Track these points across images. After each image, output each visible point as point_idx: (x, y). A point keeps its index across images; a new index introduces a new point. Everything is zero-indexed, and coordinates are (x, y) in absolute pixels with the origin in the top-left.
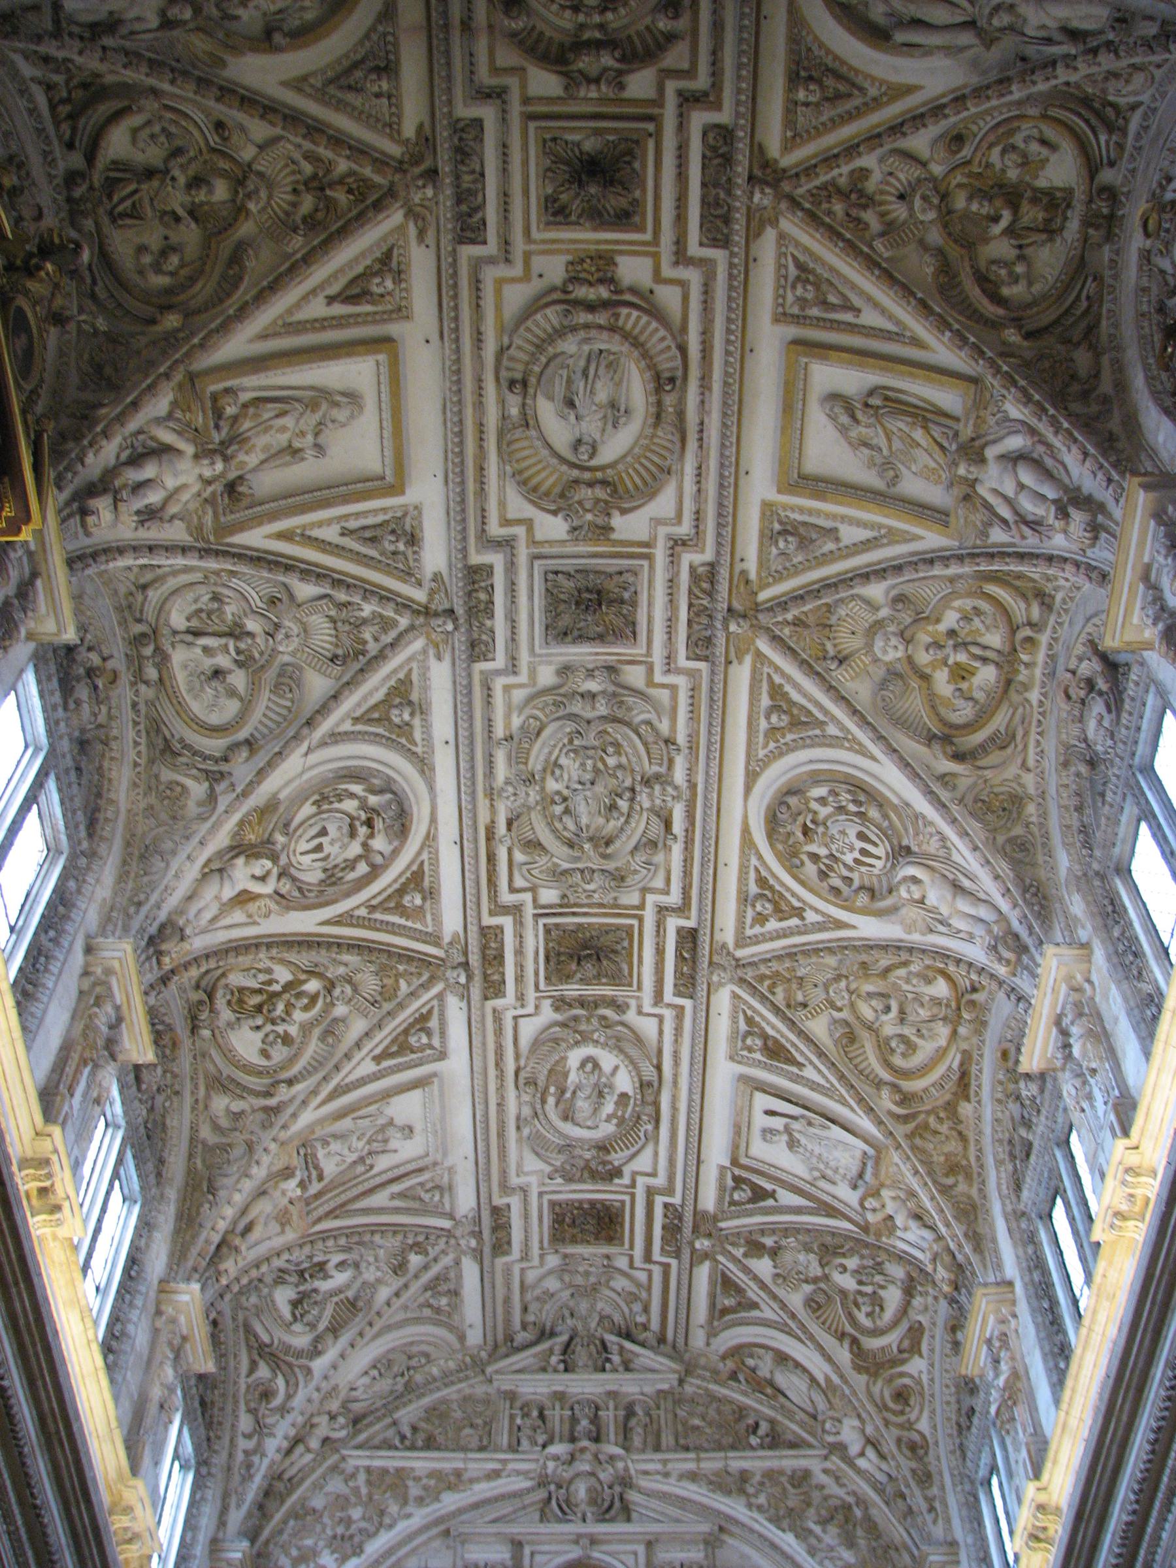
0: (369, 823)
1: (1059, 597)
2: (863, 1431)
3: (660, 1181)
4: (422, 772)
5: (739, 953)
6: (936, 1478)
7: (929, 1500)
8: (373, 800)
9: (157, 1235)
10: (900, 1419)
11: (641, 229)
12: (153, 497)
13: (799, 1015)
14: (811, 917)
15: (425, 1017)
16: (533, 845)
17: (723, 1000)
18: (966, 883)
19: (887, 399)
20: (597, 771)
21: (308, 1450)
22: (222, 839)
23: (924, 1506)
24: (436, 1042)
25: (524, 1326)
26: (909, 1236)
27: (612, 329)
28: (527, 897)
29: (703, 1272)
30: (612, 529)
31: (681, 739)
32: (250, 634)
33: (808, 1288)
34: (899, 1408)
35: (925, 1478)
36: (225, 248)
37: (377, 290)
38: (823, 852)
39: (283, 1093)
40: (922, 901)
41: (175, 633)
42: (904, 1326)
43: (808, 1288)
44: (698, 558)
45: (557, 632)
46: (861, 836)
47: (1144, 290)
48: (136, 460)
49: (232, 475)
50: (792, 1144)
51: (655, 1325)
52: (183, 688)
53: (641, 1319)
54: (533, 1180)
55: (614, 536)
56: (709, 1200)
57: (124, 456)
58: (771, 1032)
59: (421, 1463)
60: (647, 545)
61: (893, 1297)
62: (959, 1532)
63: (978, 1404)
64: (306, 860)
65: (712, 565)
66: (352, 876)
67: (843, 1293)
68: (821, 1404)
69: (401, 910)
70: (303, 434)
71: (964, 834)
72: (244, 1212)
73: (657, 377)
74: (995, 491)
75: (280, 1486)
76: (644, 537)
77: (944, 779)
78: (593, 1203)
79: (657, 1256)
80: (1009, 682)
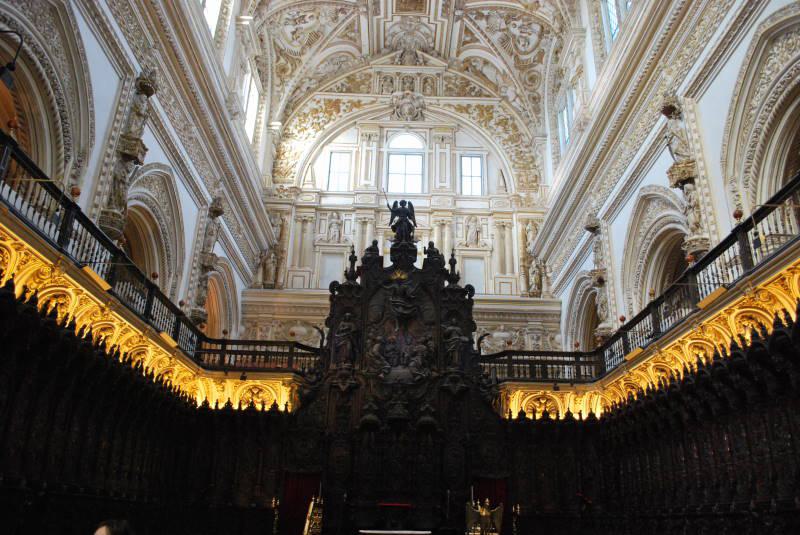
2: (516, 93)
7: (538, 119)
21: (301, 92)
25: (385, 47)
26: (544, 10)
33: (500, 34)
35: (537, 110)
42: (536, 51)
51: (437, 48)
53: (432, 45)
59: (345, 98)
61: (534, 39)
63: (563, 81)
67: (514, 36)
79: (439, 18)
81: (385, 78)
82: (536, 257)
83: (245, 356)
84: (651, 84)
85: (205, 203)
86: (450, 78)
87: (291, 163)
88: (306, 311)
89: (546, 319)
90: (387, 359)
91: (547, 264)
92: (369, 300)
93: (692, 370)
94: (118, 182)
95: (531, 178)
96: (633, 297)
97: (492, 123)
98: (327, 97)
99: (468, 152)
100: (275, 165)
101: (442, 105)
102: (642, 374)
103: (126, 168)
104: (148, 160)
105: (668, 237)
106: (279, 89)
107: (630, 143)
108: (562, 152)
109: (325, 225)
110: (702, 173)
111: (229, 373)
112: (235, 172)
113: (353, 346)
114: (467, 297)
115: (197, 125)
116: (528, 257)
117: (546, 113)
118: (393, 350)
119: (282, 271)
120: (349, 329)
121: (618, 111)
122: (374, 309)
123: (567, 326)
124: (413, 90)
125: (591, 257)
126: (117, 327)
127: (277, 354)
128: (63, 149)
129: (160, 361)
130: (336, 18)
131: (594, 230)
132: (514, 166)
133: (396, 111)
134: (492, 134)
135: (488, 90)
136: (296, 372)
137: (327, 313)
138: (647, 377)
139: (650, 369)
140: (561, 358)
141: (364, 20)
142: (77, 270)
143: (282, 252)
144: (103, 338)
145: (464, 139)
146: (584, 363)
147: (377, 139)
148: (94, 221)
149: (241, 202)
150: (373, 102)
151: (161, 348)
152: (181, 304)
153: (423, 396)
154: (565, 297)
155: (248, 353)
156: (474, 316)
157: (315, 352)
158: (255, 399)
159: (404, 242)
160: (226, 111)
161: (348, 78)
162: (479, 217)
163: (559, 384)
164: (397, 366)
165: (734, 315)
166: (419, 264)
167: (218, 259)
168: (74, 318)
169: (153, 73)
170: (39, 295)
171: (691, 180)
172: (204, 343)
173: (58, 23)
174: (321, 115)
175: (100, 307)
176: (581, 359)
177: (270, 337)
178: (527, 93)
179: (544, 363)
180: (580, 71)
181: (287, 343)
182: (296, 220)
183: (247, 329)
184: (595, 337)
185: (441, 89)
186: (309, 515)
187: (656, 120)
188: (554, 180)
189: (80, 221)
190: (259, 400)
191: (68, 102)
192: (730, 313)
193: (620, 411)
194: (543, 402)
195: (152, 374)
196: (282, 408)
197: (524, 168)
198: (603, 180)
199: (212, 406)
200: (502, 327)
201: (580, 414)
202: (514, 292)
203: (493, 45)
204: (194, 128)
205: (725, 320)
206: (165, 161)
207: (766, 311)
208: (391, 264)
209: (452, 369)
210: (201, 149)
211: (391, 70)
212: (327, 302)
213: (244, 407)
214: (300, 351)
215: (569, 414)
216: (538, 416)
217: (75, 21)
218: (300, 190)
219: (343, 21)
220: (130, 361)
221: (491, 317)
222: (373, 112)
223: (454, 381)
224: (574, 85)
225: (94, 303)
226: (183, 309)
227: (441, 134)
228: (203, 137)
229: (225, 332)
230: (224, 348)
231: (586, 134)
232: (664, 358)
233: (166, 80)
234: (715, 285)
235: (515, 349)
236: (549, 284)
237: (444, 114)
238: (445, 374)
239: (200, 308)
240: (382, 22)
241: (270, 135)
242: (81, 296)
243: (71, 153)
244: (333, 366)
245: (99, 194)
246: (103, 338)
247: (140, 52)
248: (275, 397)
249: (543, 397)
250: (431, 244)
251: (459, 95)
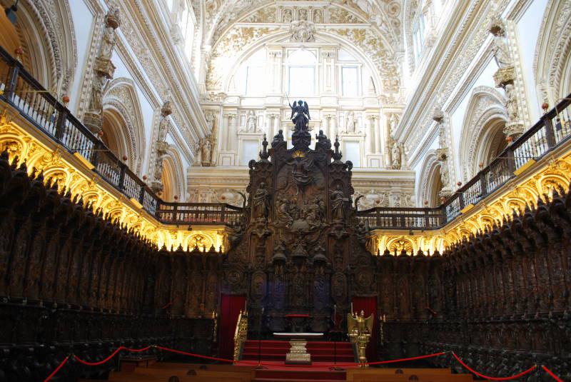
6: (401, 32)
21: (225, 23)
34: (392, 12)
35: (398, 32)
62: (406, 47)
75: (218, 33)
82: (397, 140)
83: (190, 214)
84: (483, 11)
85: (159, 106)
86: (333, 9)
88: (232, 182)
89: (403, 184)
90: (291, 215)
91: (405, 145)
92: (278, 173)
93: (509, 220)
94: (96, 92)
95: (394, 83)
96: (467, 167)
97: (365, 42)
98: (244, 26)
99: (347, 65)
100: (207, 77)
101: (328, 30)
102: (473, 223)
103: (101, 82)
104: (116, 75)
105: (496, 122)
106: (209, 21)
107: (466, 55)
108: (416, 63)
109: (244, 120)
110: (520, 76)
111: (180, 226)
112: (179, 83)
113: (266, 205)
114: (347, 170)
115: (150, 49)
116: (391, 141)
117: (405, 34)
118: (294, 208)
119: (215, 154)
120: (263, 194)
121: (458, 31)
122: (281, 180)
123: (419, 191)
124: (306, 20)
125: (437, 140)
126: (100, 195)
127: (213, 212)
128: (55, 69)
129: (131, 219)
131: (439, 119)
132: (380, 74)
133: (294, 35)
134: (365, 51)
135: (362, 18)
136: (227, 225)
137: (247, 183)
138: (477, 225)
139: (479, 220)
140: (415, 213)
142: (70, 155)
143: (214, 140)
144: (90, 203)
145: (346, 55)
146: (432, 216)
148: (80, 120)
149: (184, 105)
150: (277, 29)
151: (131, 209)
152: (144, 178)
153: (317, 240)
154: (418, 169)
155: (192, 212)
156: (353, 184)
157: (240, 210)
158: (199, 244)
159: (301, 131)
160: (170, 38)
161: (259, 11)
162: (356, 112)
163: (413, 231)
164: (297, 219)
165: (540, 180)
166: (312, 147)
167: (169, 146)
168: (70, 189)
169: (117, 11)
170: (44, 174)
171: (511, 82)
172: (161, 205)
174: (240, 39)
175: (87, 181)
176: (430, 213)
177: (208, 200)
178: (390, 19)
179: (403, 216)
181: (220, 204)
182: (224, 117)
183: (192, 195)
184: (439, 198)
185: (327, 18)
186: (238, 323)
187: (486, 38)
188: (410, 83)
189: (70, 120)
190: (202, 245)
191: (57, 32)
192: (537, 179)
193: (457, 249)
194: (402, 243)
195: (126, 228)
196: (217, 250)
197: (388, 75)
198: (446, 83)
199: (169, 249)
200: (373, 191)
201: (428, 252)
202: (381, 166)
204: (148, 51)
205: (534, 183)
206: (128, 76)
207: (564, 177)
208: (293, 146)
209: (337, 221)
210: (154, 67)
212: (247, 175)
213: (191, 250)
214: (229, 210)
215: (420, 252)
216: (399, 253)
220: (110, 219)
221: (365, 184)
222: (277, 36)
223: (339, 229)
224: (425, 12)
225: (83, 179)
226: (146, 182)
227: (327, 51)
228: (155, 57)
229: (176, 198)
230: (175, 209)
231: (434, 49)
232: (489, 211)
233: (126, 17)
234: (527, 158)
235: (382, 206)
236: (406, 160)
237: (329, 37)
238: (332, 225)
239: (158, 181)
242: (74, 174)
243: (61, 72)
244: (252, 220)
245: (82, 101)
246: (90, 203)
248: (213, 243)
249: (402, 240)
250: (321, 132)
251: (340, 22)
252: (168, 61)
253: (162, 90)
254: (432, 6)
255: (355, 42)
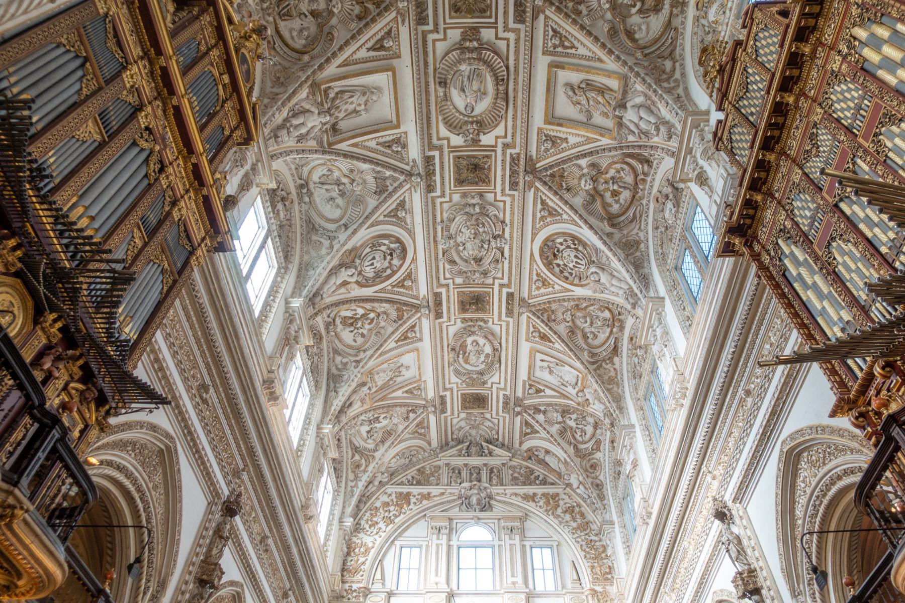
0: (391, 255)
1: (655, 163)
3: (502, 386)
4: (410, 236)
5: (530, 301)
6: (607, 497)
8: (392, 246)
9: (316, 409)
10: (593, 475)
11: (490, 17)
12: (303, 130)
13: (552, 324)
14: (557, 287)
15: (414, 326)
16: (453, 262)
17: (524, 318)
18: (615, 274)
19: (588, 84)
20: (475, 234)
22: (335, 262)
23: (602, 508)
24: (418, 335)
25: (452, 440)
26: (594, 407)
27: (479, 59)
28: (451, 281)
29: (518, 419)
30: (480, 141)
31: (508, 221)
32: (344, 184)
33: (557, 426)
35: (602, 497)
36: (326, 29)
37: (387, 45)
38: (561, 263)
39: (362, 355)
40: (599, 281)
41: (315, 183)
43: (557, 426)
44: (513, 151)
45: (460, 182)
46: (576, 257)
47: (695, 34)
48: (295, 116)
49: (333, 121)
50: (551, 372)
51: (501, 439)
52: (319, 206)
53: (496, 437)
54: (455, 386)
55: (481, 143)
56: (520, 394)
57: (290, 114)
58: (542, 330)
59: (416, 490)
60: (493, 146)
61: (589, 430)
64: (368, 269)
65: (519, 154)
66: (385, 274)
67: (571, 428)
68: (563, 469)
69: (403, 286)
70: (360, 105)
71: (615, 255)
72: (349, 399)
73: (497, 78)
74: (631, 121)
75: (364, 499)
76: (493, 143)
77: (609, 235)
78: (477, 394)
80: (634, 197)
81: (453, 469)
86: (515, 467)
87: (362, 560)
97: (559, 511)
99: (537, 543)
100: (344, 563)
106: (353, 484)
115: (273, 536)
124: (479, 481)
130: (407, 418)
133: (465, 502)
134: (560, 522)
141: (432, 419)
147: (447, 531)
150: (443, 494)
161: (419, 470)
169: (239, 495)
173: (162, 462)
174: (392, 508)
180: (635, 465)
187: (712, 523)
203: (552, 436)
204: (270, 541)
211: (459, 462)
217: (178, 459)
218: (369, 590)
219: (414, 420)
222: (441, 504)
227: (510, 524)
240: (449, 419)
241: (341, 532)
243: (151, 584)
247: (229, 478)
251: (524, 484)
252: (294, 550)
253: (280, 594)
254: (637, 467)
255: (546, 510)
